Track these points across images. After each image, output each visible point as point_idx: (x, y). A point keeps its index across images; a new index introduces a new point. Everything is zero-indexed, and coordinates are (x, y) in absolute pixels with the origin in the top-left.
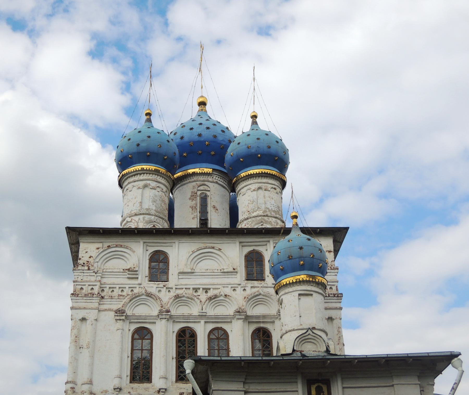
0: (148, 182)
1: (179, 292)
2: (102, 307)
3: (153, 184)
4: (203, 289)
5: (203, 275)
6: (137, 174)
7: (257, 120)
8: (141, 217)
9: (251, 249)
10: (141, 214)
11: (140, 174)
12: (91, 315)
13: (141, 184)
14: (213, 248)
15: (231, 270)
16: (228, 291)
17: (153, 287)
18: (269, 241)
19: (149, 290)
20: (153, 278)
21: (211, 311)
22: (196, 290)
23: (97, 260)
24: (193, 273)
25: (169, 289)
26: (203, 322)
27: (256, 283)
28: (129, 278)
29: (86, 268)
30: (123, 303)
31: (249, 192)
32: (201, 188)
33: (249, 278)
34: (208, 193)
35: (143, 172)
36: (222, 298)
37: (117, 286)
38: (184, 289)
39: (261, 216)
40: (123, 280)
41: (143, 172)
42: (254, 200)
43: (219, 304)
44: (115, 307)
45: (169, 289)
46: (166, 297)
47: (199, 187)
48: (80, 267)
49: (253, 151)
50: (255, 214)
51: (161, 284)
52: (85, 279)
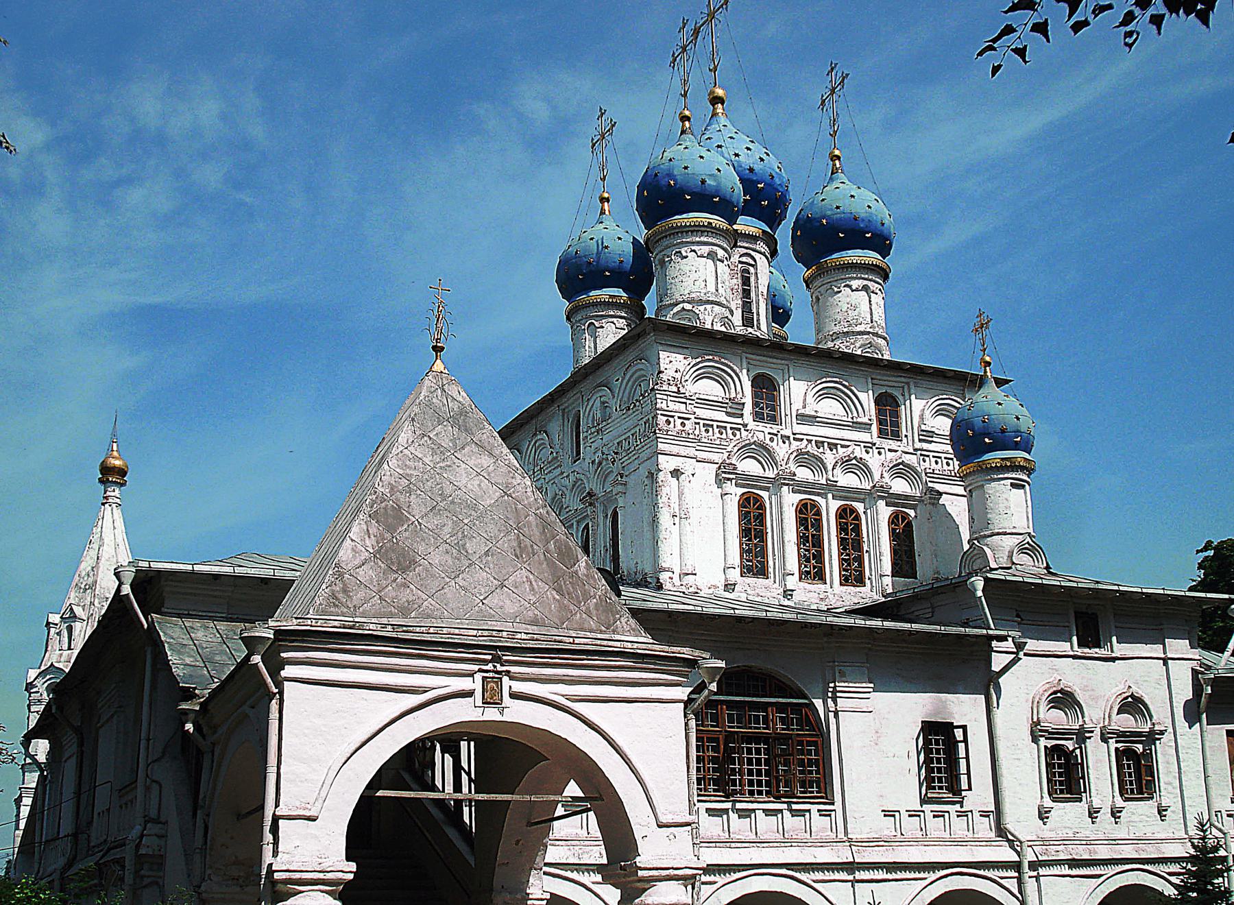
2: (701, 455)
3: (721, 253)
8: (709, 307)
12: (688, 466)
13: (705, 250)
15: (865, 420)
16: (859, 452)
17: (761, 431)
18: (908, 384)
19: (761, 436)
20: (758, 417)
21: (847, 480)
22: (819, 444)
25: (785, 438)
26: (830, 496)
27: (893, 444)
28: (728, 414)
32: (744, 259)
33: (882, 434)
34: (752, 270)
35: (710, 229)
36: (854, 462)
37: (715, 424)
38: (805, 442)
39: (869, 333)
40: (721, 416)
43: (847, 470)
44: (717, 458)
45: (785, 438)
46: (781, 451)
50: (858, 329)
52: (672, 406)
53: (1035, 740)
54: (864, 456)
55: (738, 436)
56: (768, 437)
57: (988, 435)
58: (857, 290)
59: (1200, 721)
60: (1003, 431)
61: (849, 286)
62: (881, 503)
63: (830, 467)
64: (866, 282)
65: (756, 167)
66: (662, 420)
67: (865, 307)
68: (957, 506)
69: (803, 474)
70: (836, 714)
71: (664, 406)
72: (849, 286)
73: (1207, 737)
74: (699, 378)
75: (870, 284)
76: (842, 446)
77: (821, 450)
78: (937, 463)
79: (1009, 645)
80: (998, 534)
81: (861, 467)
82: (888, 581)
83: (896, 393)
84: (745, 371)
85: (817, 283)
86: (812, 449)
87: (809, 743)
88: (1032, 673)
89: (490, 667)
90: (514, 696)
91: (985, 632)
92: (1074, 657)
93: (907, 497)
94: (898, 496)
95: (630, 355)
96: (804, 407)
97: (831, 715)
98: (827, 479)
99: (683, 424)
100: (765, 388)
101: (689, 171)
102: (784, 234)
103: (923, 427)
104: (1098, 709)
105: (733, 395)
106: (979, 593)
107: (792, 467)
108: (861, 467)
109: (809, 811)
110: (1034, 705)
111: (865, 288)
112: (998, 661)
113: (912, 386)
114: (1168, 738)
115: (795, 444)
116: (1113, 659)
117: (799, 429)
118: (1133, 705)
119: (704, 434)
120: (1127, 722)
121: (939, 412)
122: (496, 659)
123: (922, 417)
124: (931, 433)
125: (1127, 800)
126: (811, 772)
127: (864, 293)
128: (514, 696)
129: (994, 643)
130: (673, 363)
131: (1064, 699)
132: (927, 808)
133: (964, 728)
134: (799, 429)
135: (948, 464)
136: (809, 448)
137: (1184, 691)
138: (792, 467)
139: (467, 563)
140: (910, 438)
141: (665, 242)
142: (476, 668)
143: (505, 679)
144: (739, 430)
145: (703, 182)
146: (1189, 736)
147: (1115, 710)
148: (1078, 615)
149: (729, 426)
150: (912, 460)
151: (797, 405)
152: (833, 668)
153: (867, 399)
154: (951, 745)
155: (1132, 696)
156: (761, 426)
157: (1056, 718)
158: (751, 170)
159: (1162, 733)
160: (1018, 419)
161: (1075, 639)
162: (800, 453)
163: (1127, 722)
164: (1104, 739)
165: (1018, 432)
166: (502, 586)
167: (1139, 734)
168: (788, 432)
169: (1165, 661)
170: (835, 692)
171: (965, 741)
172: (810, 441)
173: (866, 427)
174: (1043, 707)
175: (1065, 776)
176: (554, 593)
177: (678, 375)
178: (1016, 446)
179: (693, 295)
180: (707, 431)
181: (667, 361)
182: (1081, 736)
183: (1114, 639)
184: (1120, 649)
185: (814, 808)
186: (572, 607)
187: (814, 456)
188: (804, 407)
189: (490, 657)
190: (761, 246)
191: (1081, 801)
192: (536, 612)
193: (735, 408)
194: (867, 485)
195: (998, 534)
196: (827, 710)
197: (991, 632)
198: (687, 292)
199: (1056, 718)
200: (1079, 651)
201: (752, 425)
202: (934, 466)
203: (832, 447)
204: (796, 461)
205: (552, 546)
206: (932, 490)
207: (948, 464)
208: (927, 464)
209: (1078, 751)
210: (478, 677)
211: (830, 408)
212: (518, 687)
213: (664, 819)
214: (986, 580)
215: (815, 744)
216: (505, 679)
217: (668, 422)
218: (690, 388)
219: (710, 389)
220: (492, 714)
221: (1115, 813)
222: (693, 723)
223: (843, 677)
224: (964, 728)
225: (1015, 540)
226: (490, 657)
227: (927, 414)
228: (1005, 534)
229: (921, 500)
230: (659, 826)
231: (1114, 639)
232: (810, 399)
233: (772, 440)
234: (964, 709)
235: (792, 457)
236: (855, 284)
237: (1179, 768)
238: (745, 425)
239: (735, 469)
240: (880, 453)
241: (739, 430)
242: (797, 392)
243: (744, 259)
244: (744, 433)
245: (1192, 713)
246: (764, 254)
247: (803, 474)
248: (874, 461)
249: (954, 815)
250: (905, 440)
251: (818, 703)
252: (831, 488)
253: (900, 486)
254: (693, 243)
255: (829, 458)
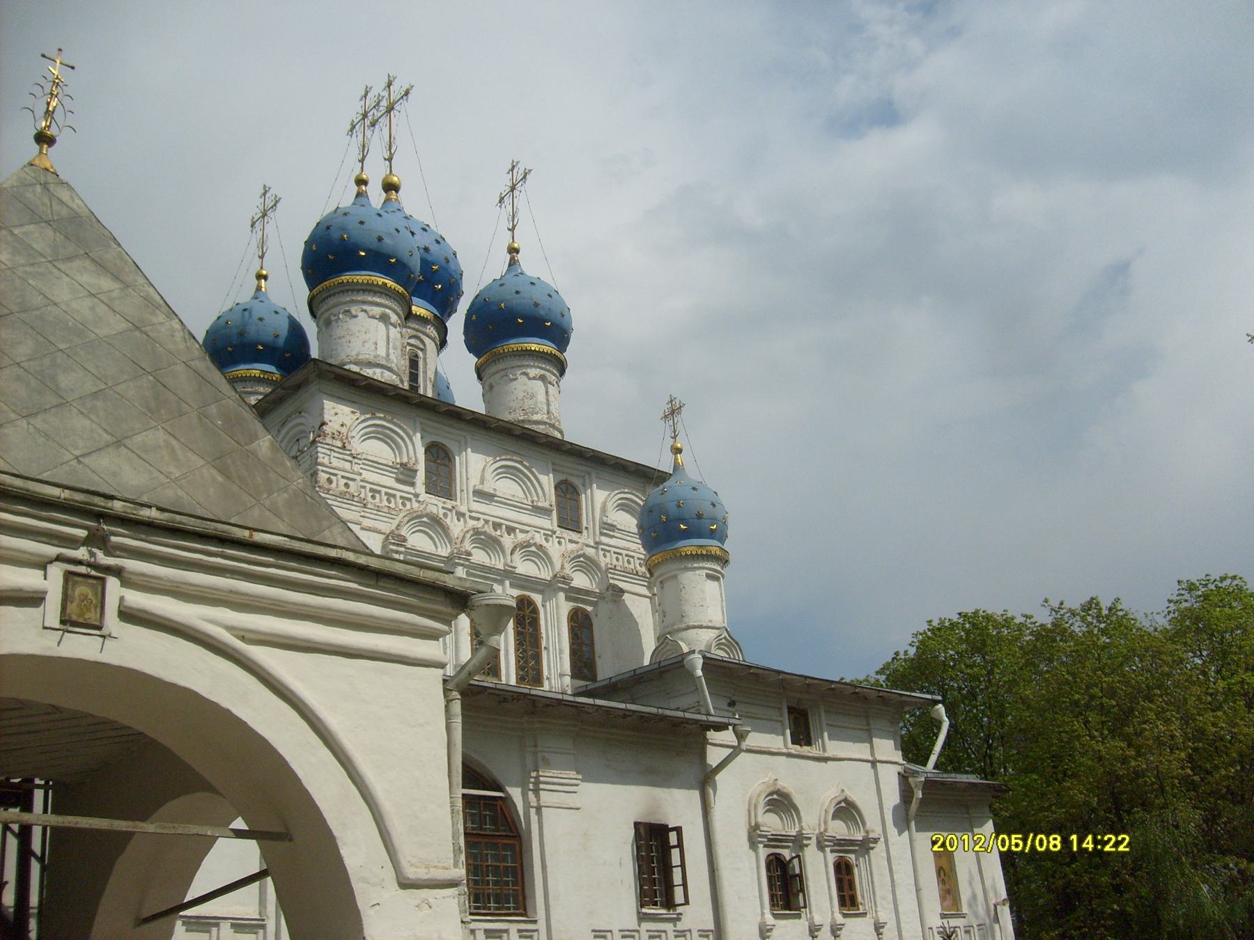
0: (388, 311)
1: (479, 524)
3: (394, 318)
4: (507, 527)
5: (506, 503)
6: (370, 291)
7: (520, 257)
9: (563, 477)
10: (382, 366)
11: (375, 293)
13: (377, 311)
14: (521, 463)
16: (539, 538)
17: (436, 505)
18: (589, 474)
19: (434, 510)
21: (525, 568)
22: (497, 526)
23: (354, 434)
24: (494, 496)
25: (460, 515)
26: (507, 583)
27: (574, 536)
28: (398, 480)
29: (339, 444)
30: (396, 523)
31: (524, 378)
32: (412, 341)
34: (420, 354)
35: (383, 291)
36: (533, 549)
37: (383, 490)
39: (545, 423)
40: (391, 482)
41: (383, 291)
42: (531, 396)
44: (386, 527)
45: (460, 515)
46: (456, 528)
47: (410, 337)
48: (329, 440)
49: (542, 313)
50: (535, 417)
51: (449, 504)
52: (335, 463)
53: (753, 845)
54: (544, 543)
55: (408, 506)
56: (441, 512)
57: (683, 520)
58: (534, 378)
59: (908, 828)
60: (699, 516)
61: (526, 374)
62: (562, 595)
63: (508, 552)
64: (543, 372)
65: (431, 248)
66: (323, 477)
67: (541, 397)
68: (640, 607)
69: (479, 557)
70: (539, 809)
71: (326, 461)
72: (526, 374)
73: (917, 845)
74: (367, 437)
75: (548, 374)
76: (522, 531)
77: (498, 533)
78: (617, 559)
79: (728, 736)
80: (694, 627)
81: (540, 554)
82: (567, 680)
83: (577, 482)
84: (418, 435)
85: (493, 369)
86: (489, 529)
87: (505, 847)
88: (752, 768)
89: (82, 553)
90: (129, 615)
91: (704, 718)
92: (789, 755)
93: (587, 592)
94: (579, 591)
95: (287, 408)
96: (482, 483)
97: (533, 811)
98: (506, 564)
99: (347, 485)
100: (439, 457)
101: (364, 226)
102: (456, 324)
103: (605, 519)
104: (813, 817)
105: (405, 460)
106: (699, 673)
107: (468, 546)
108: (540, 554)
109: (506, 931)
110: (751, 809)
111: (542, 378)
112: (714, 756)
113: (594, 475)
114: (880, 846)
115: (471, 523)
116: (826, 760)
117: (476, 506)
118: (846, 810)
119: (370, 499)
120: (839, 829)
121: (624, 507)
122: (97, 540)
123: (604, 510)
124: (612, 527)
125: (845, 916)
126: (507, 883)
127: (540, 383)
128: (129, 615)
129: (712, 735)
130: (339, 414)
131: (780, 802)
132: (646, 925)
133: (678, 830)
134: (476, 506)
135: (629, 562)
136: (486, 528)
137: (892, 796)
138: (468, 546)
139: (55, 401)
140: (591, 531)
141: (332, 301)
142: (52, 550)
143: (112, 583)
144: (410, 500)
145: (380, 239)
146: (899, 842)
147: (830, 816)
148: (791, 710)
149: (399, 494)
150: (591, 552)
151: (474, 482)
152: (535, 754)
153: (548, 481)
154: (665, 849)
155: (846, 800)
156: (432, 499)
157: (772, 823)
158: (426, 249)
159: (876, 841)
160: (714, 505)
161: (788, 732)
162: (476, 532)
163: (839, 829)
164: (821, 847)
165: (714, 520)
166: (118, 443)
167: (852, 842)
168: (463, 509)
169: (874, 763)
170: (537, 783)
171: (680, 845)
172: (487, 522)
173: (545, 512)
174: (761, 810)
175: (785, 887)
176: (214, 472)
177: (344, 430)
178: (712, 534)
179: (361, 357)
180: (374, 497)
181: (333, 412)
182: (799, 842)
183: (826, 734)
184: (835, 747)
185: (513, 928)
186: (246, 497)
187: (490, 537)
188: (482, 483)
189: (82, 533)
190: (431, 330)
191: (799, 916)
192: (180, 493)
193: (406, 473)
194: (546, 575)
195: (694, 627)
196: (527, 806)
197: (711, 719)
198: (354, 353)
199: (772, 823)
200: (795, 749)
201: (424, 496)
202: (615, 562)
203: (511, 530)
204: (473, 541)
205: (213, 409)
206: (614, 586)
207: (629, 562)
208: (608, 560)
209: (796, 861)
210: (57, 571)
211: (508, 488)
212: (137, 599)
213: (412, 873)
214: (704, 657)
215: (512, 848)
216: (112, 583)
217: (330, 481)
218: (357, 446)
219: (378, 450)
220: (80, 646)
221: (835, 930)
222: (457, 707)
223: (548, 764)
224: (678, 830)
225: (712, 634)
226: (82, 533)
227: (610, 506)
228: (701, 627)
229: (601, 596)
230: (406, 884)
231: (826, 734)
232: (489, 475)
233: (445, 515)
234: (677, 806)
235: (468, 536)
236: (533, 372)
237: (893, 881)
238: (416, 496)
239: (405, 540)
240: (559, 543)
241: (410, 500)
242: (474, 465)
243: (412, 341)
244: (415, 505)
245: (903, 818)
246: (433, 339)
247: (479, 557)
248: (554, 549)
249: (671, 935)
250: (585, 532)
251: (515, 793)
252: (508, 574)
253: (581, 581)
254: (364, 302)
255: (508, 541)
